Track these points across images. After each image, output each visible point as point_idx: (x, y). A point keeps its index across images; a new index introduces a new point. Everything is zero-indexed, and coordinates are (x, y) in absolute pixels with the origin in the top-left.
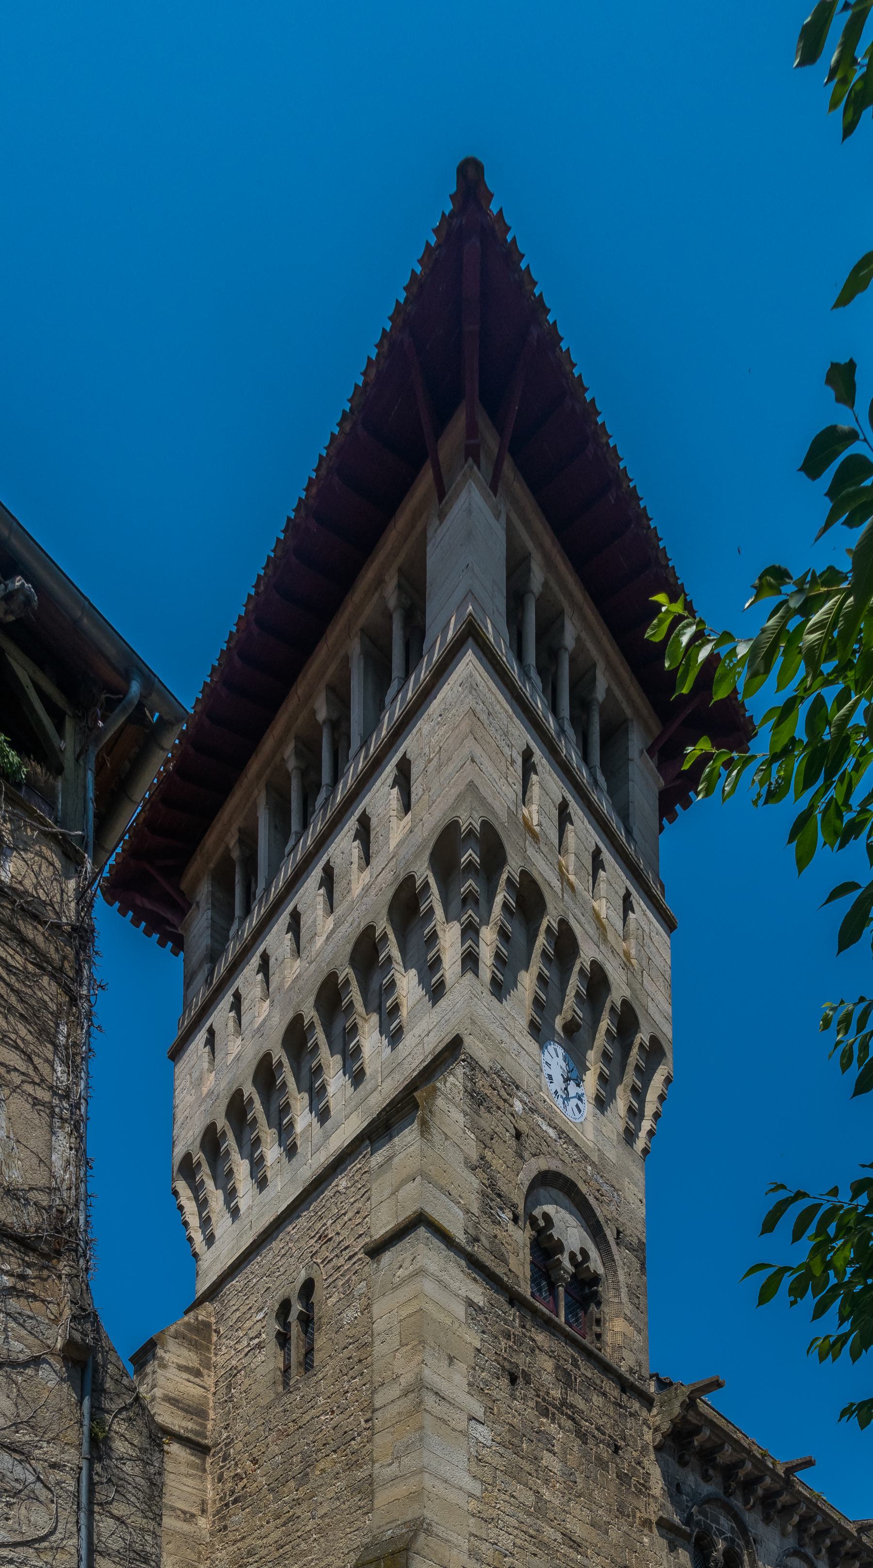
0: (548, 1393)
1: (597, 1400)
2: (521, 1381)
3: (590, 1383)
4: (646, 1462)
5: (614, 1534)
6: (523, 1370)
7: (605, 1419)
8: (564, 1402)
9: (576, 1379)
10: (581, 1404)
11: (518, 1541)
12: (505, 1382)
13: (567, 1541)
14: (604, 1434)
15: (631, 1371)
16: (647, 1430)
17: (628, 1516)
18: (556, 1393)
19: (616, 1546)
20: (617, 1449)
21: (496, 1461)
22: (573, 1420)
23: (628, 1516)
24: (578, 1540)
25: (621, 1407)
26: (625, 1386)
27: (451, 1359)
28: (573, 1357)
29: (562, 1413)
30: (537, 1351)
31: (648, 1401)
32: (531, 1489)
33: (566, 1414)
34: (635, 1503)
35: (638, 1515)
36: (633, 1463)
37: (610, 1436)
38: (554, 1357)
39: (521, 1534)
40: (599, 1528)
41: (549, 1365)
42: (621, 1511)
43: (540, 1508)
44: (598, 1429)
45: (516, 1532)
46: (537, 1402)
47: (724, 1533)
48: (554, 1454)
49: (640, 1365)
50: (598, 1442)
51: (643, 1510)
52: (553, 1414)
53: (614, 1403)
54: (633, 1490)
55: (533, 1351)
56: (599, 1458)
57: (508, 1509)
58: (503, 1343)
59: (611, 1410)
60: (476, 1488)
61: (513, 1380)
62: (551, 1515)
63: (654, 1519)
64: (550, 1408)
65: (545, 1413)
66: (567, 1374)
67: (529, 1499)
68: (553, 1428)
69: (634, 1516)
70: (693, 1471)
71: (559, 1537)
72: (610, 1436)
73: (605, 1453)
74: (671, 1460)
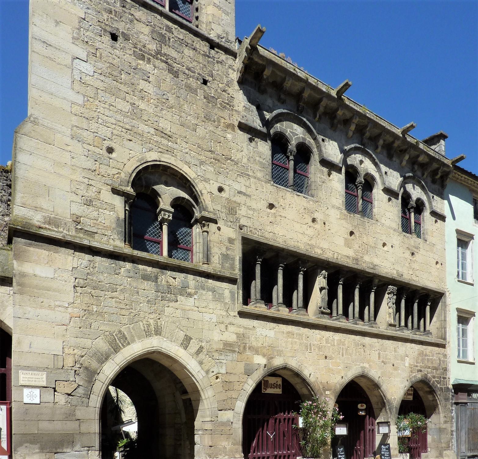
0: (144, 46)
1: (187, 52)
2: (120, 39)
3: (182, 42)
4: (230, 90)
5: (201, 131)
6: (123, 32)
7: (195, 64)
8: (158, 52)
9: (169, 39)
10: (174, 54)
11: (115, 132)
12: (107, 38)
13: (160, 133)
14: (194, 72)
15: (219, 36)
16: (232, 71)
17: (214, 121)
18: (152, 47)
19: (203, 138)
20: (205, 82)
21: (98, 84)
22: (166, 63)
23: (214, 121)
24: (169, 133)
25: (209, 57)
26: (213, 45)
27: (57, 23)
28: (167, 26)
29: (157, 59)
30: (135, 22)
31: (234, 55)
32: (128, 102)
33: (161, 59)
34: (220, 113)
35: (223, 121)
36: (219, 91)
37: (199, 74)
38: (151, 26)
39: (117, 128)
40: (188, 127)
41: (146, 30)
42: (207, 118)
43: (135, 113)
44: (189, 69)
45: (114, 126)
46: (134, 51)
47: (297, 135)
48: (149, 82)
49: (227, 34)
50: (188, 77)
51: (227, 118)
52: (149, 59)
53: (203, 55)
54: (219, 106)
55: (131, 21)
56: (189, 87)
57: (107, 113)
58: (106, 16)
59: (201, 59)
60: (80, 99)
61: (114, 37)
62: (145, 118)
63: (236, 124)
64: (146, 55)
65: (142, 58)
66: (163, 36)
67: (127, 107)
68: (149, 67)
69: (219, 122)
70: (271, 97)
71: (152, 131)
72: (199, 74)
73: (195, 83)
74: (252, 90)
